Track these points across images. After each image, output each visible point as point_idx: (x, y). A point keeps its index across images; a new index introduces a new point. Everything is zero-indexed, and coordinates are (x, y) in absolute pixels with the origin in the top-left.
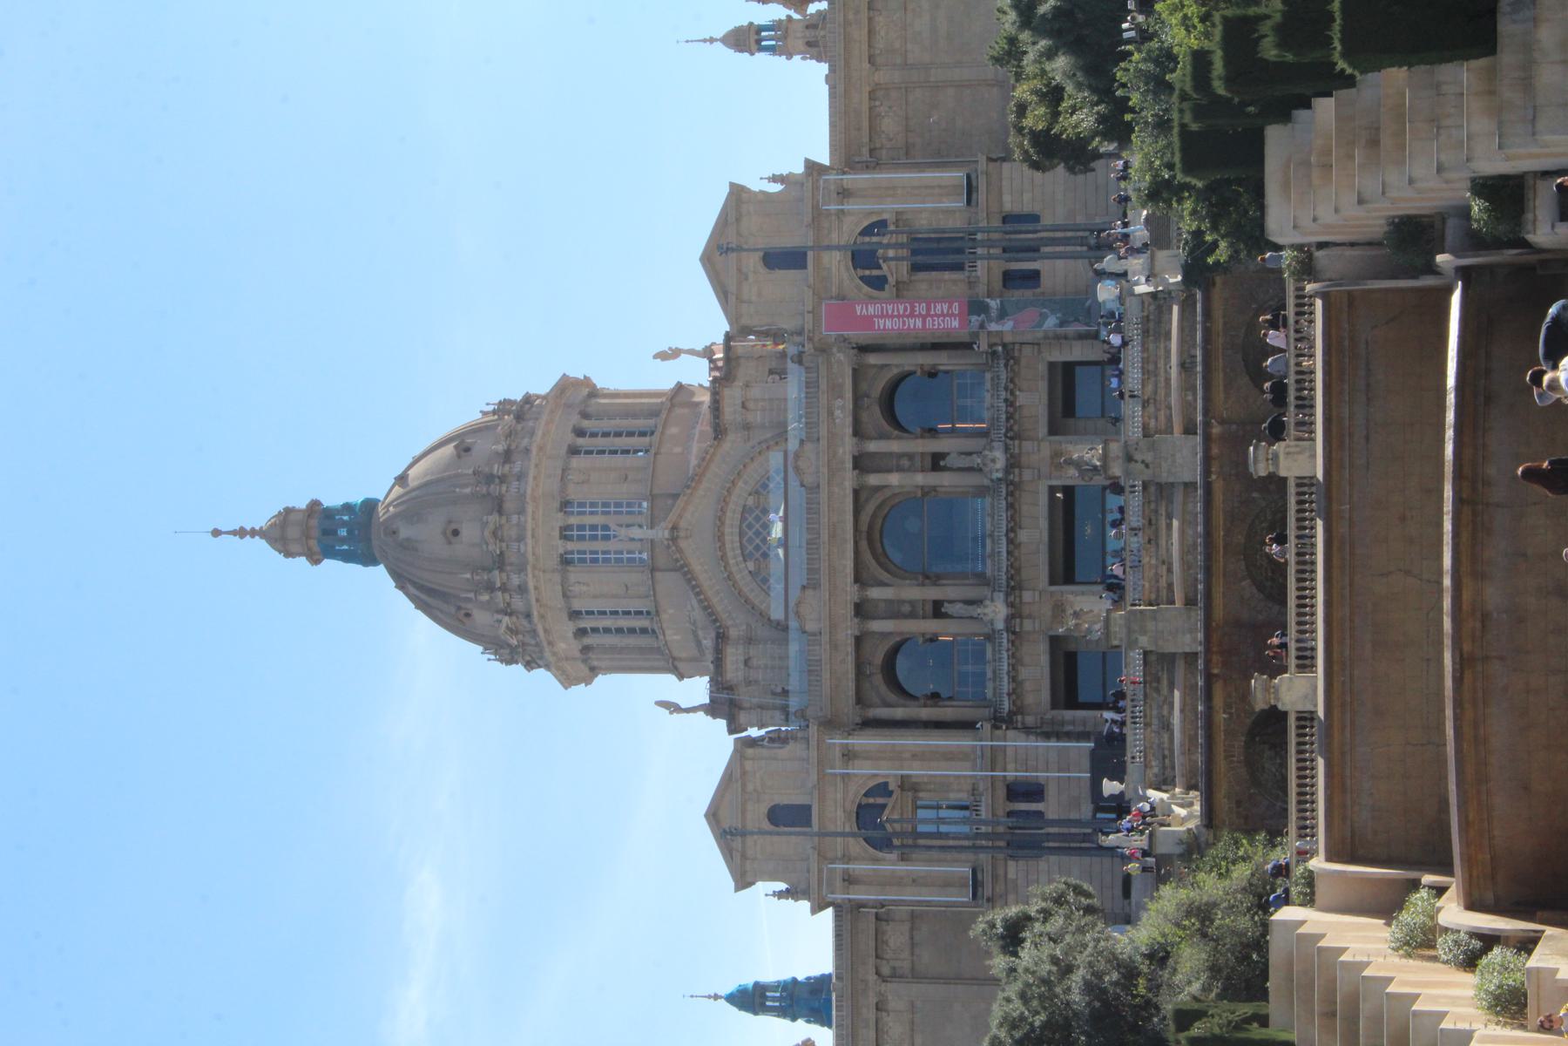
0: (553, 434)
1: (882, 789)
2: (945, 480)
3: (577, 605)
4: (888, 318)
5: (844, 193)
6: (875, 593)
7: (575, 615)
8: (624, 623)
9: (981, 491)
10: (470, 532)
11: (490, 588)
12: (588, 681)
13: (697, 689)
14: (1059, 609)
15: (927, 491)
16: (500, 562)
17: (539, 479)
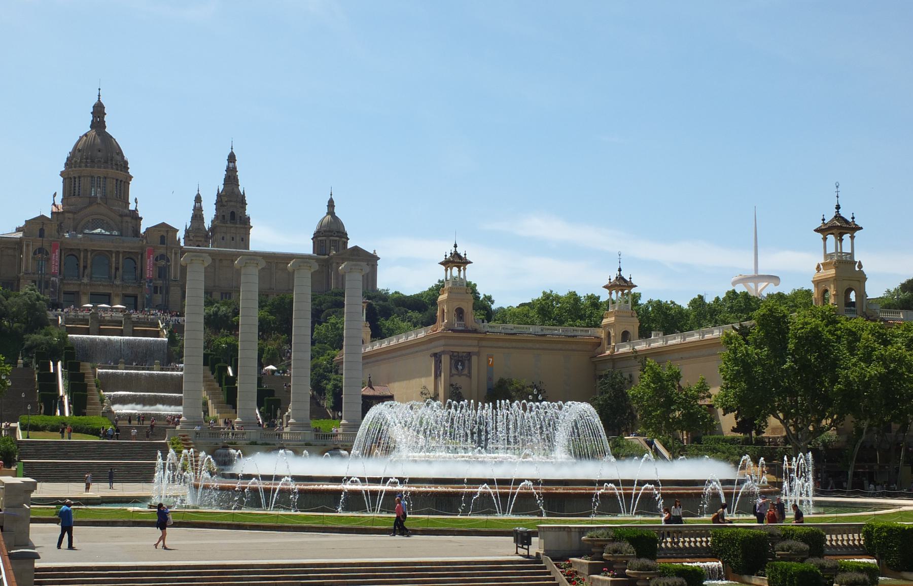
0: (120, 175)
1: (47, 254)
2: (113, 271)
3: (82, 179)
4: (149, 262)
5: (176, 254)
6: (89, 254)
7: (79, 177)
8: (77, 188)
9: (110, 278)
10: (100, 154)
11: (87, 158)
12: (61, 175)
13: (58, 201)
14: (85, 294)
15: (110, 267)
16: (93, 161)
17: (111, 172)
